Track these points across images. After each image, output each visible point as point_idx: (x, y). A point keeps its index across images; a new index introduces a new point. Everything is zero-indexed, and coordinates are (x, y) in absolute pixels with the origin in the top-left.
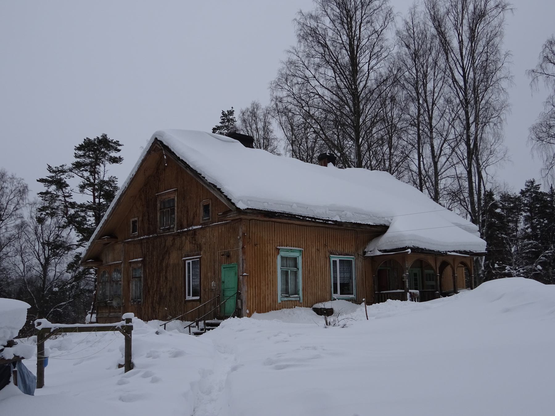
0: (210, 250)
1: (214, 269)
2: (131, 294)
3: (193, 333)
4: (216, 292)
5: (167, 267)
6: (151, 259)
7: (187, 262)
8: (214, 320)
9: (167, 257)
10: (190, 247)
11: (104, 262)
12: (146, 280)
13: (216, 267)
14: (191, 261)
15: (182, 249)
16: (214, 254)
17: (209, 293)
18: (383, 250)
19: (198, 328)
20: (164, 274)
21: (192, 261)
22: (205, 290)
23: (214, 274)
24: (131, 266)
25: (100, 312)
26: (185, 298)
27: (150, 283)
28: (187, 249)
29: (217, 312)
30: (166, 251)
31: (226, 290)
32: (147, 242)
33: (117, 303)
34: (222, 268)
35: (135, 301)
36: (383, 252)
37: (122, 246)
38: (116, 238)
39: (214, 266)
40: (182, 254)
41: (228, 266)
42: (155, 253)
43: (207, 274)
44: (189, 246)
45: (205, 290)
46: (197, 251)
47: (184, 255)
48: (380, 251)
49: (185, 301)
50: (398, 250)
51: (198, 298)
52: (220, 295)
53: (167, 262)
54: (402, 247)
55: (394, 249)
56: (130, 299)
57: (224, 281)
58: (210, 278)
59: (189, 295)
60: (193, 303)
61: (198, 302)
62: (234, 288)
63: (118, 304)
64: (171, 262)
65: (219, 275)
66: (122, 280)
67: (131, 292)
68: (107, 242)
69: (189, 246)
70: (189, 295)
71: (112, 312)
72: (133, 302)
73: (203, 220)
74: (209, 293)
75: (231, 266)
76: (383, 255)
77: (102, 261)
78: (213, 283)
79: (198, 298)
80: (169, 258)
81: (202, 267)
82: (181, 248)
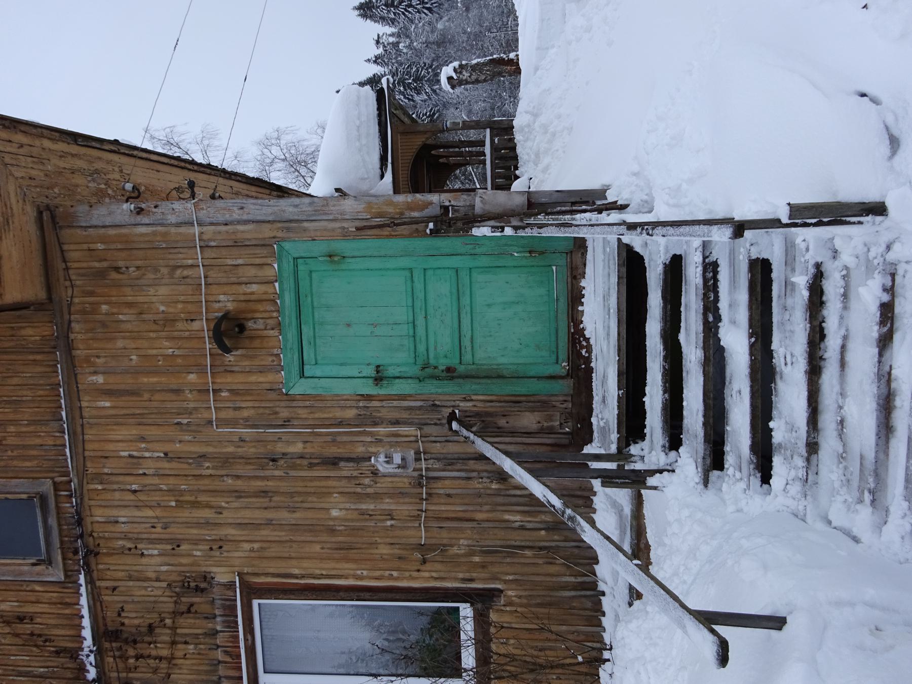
0: (208, 506)
1: (311, 466)
3: (706, 482)
13: (298, 448)
16: (226, 461)
18: (381, 169)
21: (265, 672)
23: (333, 462)
29: (550, 431)
31: (421, 348)
34: (300, 388)
36: (386, 169)
43: (332, 531)
46: (215, 617)
48: (382, 176)
50: (383, 118)
51: (466, 611)
52: (452, 417)
54: (376, 106)
55: (380, 131)
57: (370, 371)
58: (360, 497)
62: (411, 270)
73: (49, 562)
75: (289, 299)
76: (393, 163)
79: (466, 611)
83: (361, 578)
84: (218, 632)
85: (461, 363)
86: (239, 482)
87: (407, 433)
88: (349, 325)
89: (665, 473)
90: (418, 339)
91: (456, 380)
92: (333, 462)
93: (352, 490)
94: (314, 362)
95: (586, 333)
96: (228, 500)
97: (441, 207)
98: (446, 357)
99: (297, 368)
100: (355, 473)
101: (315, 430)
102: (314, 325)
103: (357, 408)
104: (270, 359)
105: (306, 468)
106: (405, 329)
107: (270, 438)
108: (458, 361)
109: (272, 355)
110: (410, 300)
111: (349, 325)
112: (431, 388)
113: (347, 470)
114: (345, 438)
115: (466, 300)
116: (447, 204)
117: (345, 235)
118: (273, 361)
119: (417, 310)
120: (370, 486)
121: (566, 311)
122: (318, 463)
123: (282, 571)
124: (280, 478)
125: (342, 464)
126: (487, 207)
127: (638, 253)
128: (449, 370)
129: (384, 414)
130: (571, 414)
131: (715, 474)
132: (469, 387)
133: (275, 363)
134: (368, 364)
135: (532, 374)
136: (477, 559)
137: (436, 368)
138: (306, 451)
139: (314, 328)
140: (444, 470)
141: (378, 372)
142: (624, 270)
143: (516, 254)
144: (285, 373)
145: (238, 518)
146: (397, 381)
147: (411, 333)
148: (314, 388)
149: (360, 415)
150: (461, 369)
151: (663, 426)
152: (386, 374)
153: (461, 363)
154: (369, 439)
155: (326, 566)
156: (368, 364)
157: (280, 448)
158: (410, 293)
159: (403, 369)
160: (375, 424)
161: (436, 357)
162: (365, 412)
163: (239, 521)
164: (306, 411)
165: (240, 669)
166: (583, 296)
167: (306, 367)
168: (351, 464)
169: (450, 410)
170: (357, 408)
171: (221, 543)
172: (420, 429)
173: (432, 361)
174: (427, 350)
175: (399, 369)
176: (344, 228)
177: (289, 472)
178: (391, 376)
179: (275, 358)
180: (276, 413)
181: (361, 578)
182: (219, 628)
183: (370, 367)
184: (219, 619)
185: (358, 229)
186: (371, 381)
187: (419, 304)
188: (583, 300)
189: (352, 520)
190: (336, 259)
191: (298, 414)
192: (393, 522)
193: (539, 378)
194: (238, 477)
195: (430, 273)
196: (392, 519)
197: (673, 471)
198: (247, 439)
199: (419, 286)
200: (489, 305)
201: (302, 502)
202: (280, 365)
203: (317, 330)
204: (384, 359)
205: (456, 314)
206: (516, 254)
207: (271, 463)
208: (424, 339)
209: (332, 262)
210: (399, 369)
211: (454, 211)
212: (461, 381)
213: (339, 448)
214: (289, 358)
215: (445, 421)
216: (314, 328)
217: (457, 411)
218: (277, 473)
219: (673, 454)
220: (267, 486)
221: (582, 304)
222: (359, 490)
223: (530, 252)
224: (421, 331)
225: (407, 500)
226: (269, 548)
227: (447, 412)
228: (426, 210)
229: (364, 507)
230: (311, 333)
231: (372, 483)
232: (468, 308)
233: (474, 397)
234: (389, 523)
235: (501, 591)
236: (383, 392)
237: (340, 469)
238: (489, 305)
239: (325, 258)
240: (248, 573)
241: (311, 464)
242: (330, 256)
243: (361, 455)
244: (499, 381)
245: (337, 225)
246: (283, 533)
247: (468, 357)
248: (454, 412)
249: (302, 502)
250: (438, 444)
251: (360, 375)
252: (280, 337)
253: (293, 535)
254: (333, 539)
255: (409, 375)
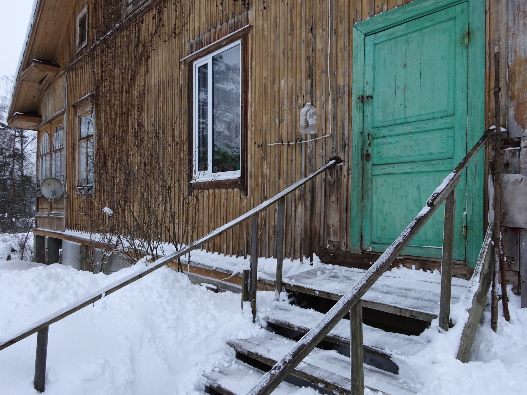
1: (308, 59)
2: (77, 173)
3: (230, 344)
4: (319, 150)
5: (142, 95)
6: (110, 86)
7: (197, 64)
8: (306, 261)
9: (143, 69)
10: (206, 14)
11: (43, 118)
12: (99, 138)
13: (319, 46)
14: (208, 60)
15: (181, 33)
17: (280, 154)
19: (254, 312)
20: (136, 117)
22: (263, 146)
23: (310, 75)
24: (76, 114)
25: (40, 207)
26: (190, 177)
27: (106, 145)
28: (197, 25)
30: (142, 54)
31: (385, 132)
32: (102, 51)
33: (52, 191)
34: (357, 36)
35: (83, 188)
37: (65, 79)
38: (58, 66)
39: (311, 46)
40: (181, 47)
41: (399, 16)
42: (117, 72)
43: (274, 83)
44: (203, 12)
45: (263, 146)
46: (234, 18)
47: (187, 47)
49: (192, 188)
51: (235, 175)
53: (142, 83)
56: (76, 184)
57: (368, 91)
58: (290, 98)
59: (203, 167)
60: (215, 193)
61: (236, 190)
62: (453, 115)
63: (54, 193)
64: (153, 79)
65: (334, 75)
66: (65, 146)
67: (77, 168)
68: (41, 75)
69: (203, 12)
70: (203, 167)
71: (54, 208)
72: (80, 189)
74: (280, 154)
77: (41, 117)
78: (304, 110)
79: (235, 175)
80: (147, 70)
81: (254, 64)
82: (178, 31)
83: (251, 107)
84: (228, 22)
85: (373, 165)
86: (299, 8)
87: (328, 127)
88: (405, 65)
89: (252, 315)
90: (392, 128)
91: (361, 162)
92: (310, 75)
93: (294, 92)
94: (376, 42)
95: (395, 268)
96: (289, 5)
97: (519, 138)
98: (378, 153)
99: (372, 29)
100: (304, 92)
101: (329, 56)
102: (407, 34)
103: (344, 86)
104: (380, 4)
105: (307, 55)
106: (400, 116)
107: (324, 23)
108: (375, 163)
109: (382, 5)
110: (426, 117)
111: (405, 65)
112: (356, 143)
113: (306, 85)
114: (324, 80)
115: (423, 167)
116: (523, 144)
117: (490, 43)
118: (378, 7)
119: (416, 125)
120: (296, 104)
121: (412, 254)
122: (310, 64)
123: (254, 55)
124: (301, 38)
125: (310, 81)
126: (510, 186)
127: (422, 331)
128: (368, 155)
129: (340, 107)
130: (339, 249)
131: (234, 353)
132: (356, 172)
133: (376, 9)
134: (374, 89)
135: (364, 222)
136: (260, 180)
137: (370, 144)
138: (317, 52)
139: (403, 35)
140: (306, 156)
141: (367, 98)
142: (407, 315)
143: (465, 213)
144: (368, 20)
145: (279, 14)
146: (361, 114)
147: (398, 122)
148: (357, 47)
149: (339, 89)
150: (369, 166)
151: (279, 321)
152: (366, 104)
153: (373, 165)
154: (324, 99)
155: (257, 83)
156: (374, 89)
157: (319, 32)
158: (431, 117)
159: (369, 118)
160: (333, 101)
161: (378, 145)
162: (341, 92)
163: (278, 16)
164: (342, 45)
165: (214, 41)
166: (425, 270)
167: (372, 36)
168: (309, 88)
169: (342, 159)
170: (344, 86)
171: (267, 8)
172: (330, 136)
173: (375, 142)
174: (383, 137)
175: (369, 115)
176: (499, 40)
177: (304, 43)
178: (365, 109)
179: (380, 8)
180: (341, 22)
181: (251, 107)
182: (229, 22)
183: (371, 90)
184: (233, 20)
185: (497, 55)
186: (361, 93)
187: (421, 126)
188: (421, 270)
189: (279, 95)
190: (466, 40)
191: (340, 40)
192: (278, 123)
193: (361, 228)
194: (301, 7)
195: (450, 133)
196: (280, 123)
197: (254, 322)
198: (324, 4)
199: (438, 124)
200: (418, 188)
201: (288, 57)
202: (374, 14)
203: (402, 38)
204: (377, 102)
205: (412, 159)
206: (465, 213)
207: (310, 28)
208: (392, 133)
209: (463, 37)
210: (369, 115)
211: (513, 153)
212: (361, 166)
213: (319, 77)
214: (380, 21)
215: (335, 155)
216: (403, 35)
217: (342, 164)
218: (304, 34)
219: (265, 324)
220: (297, 29)
221: (418, 269)
222: (294, 97)
223: (466, 227)
224: (399, 130)
225: (290, 131)
226: (265, 42)
227: (341, 156)
228: (515, 123)
229: (285, 102)
230: (399, 34)
231: (299, 105)
232: (416, 170)
233: (350, 176)
234: (277, 121)
235: (246, 196)
236: (354, 104)
237: (306, 80)
238: (418, 188)
239: (467, 29)
240: (252, 31)
241: (310, 58)
242: (468, 34)
243: (314, 94)
244: (360, 196)
245: (503, 33)
246: (272, 49)
247: (377, 171)
248: (341, 161)
249: (288, 57)
250: (321, 151)
251: (365, 83)
252: (396, 7)
253: (271, 57)
254: (269, 84)
255: (365, 123)
